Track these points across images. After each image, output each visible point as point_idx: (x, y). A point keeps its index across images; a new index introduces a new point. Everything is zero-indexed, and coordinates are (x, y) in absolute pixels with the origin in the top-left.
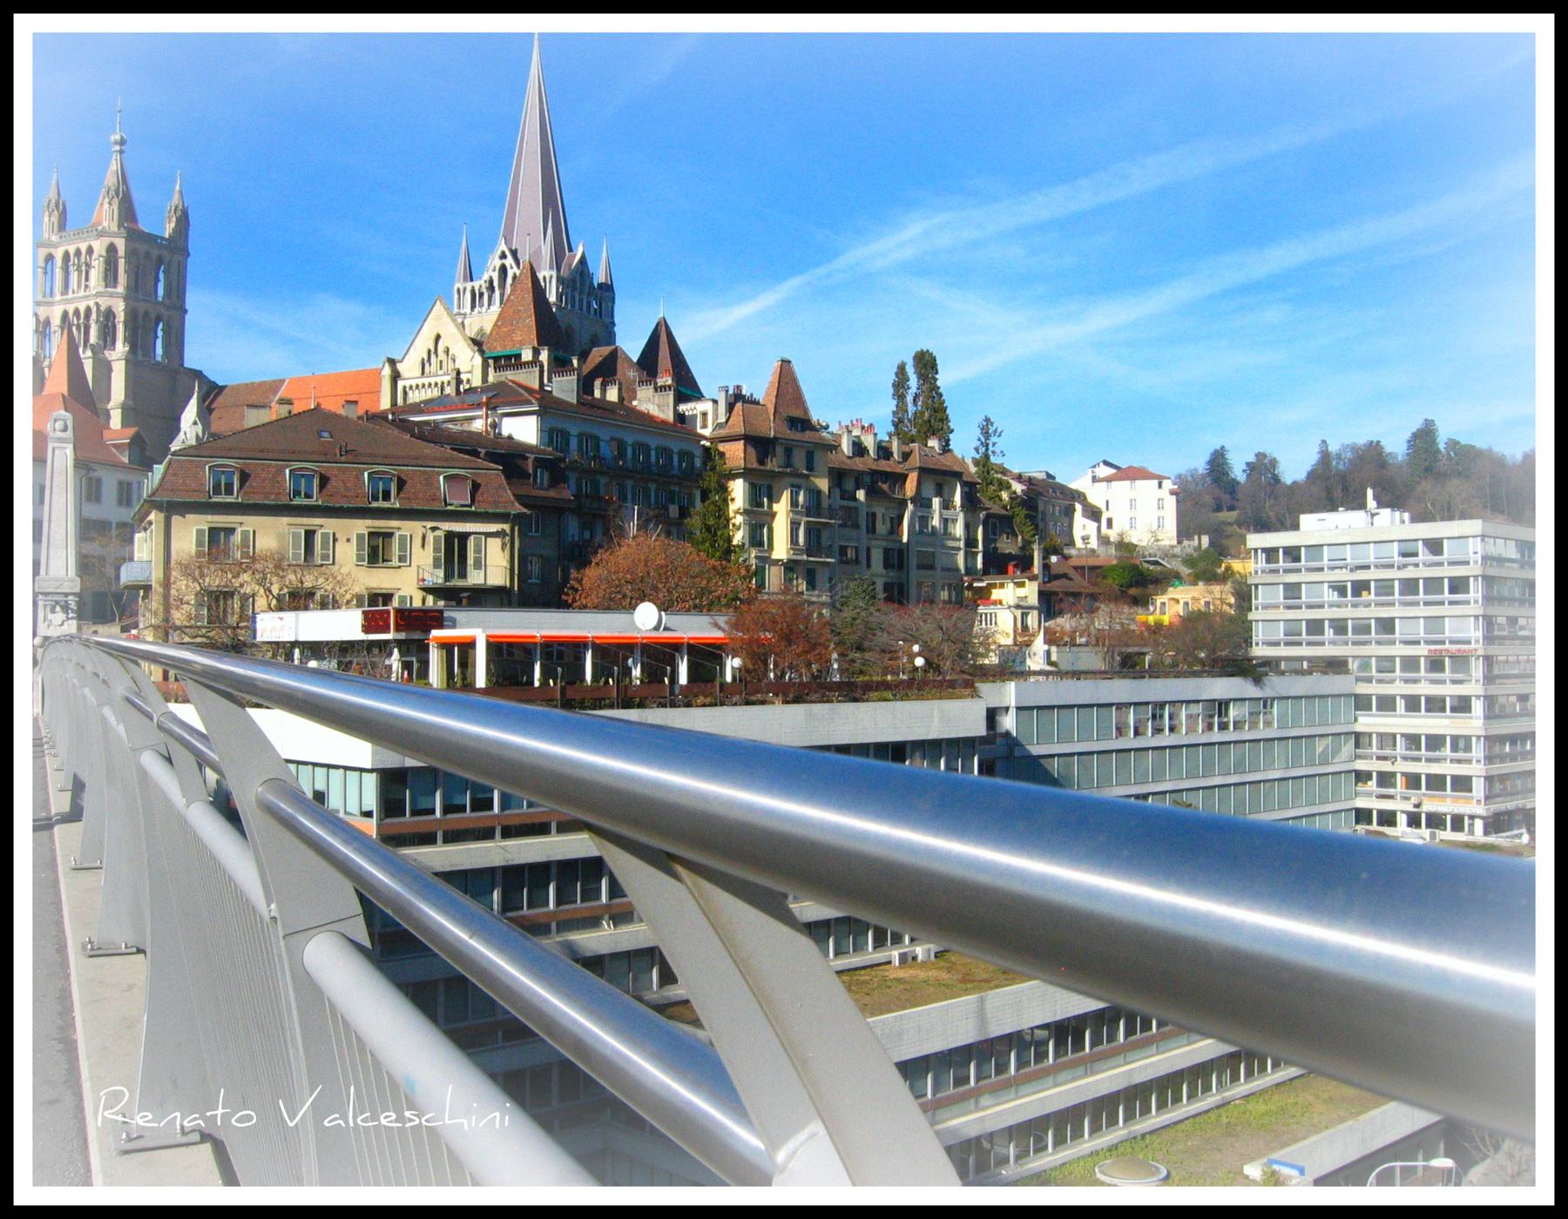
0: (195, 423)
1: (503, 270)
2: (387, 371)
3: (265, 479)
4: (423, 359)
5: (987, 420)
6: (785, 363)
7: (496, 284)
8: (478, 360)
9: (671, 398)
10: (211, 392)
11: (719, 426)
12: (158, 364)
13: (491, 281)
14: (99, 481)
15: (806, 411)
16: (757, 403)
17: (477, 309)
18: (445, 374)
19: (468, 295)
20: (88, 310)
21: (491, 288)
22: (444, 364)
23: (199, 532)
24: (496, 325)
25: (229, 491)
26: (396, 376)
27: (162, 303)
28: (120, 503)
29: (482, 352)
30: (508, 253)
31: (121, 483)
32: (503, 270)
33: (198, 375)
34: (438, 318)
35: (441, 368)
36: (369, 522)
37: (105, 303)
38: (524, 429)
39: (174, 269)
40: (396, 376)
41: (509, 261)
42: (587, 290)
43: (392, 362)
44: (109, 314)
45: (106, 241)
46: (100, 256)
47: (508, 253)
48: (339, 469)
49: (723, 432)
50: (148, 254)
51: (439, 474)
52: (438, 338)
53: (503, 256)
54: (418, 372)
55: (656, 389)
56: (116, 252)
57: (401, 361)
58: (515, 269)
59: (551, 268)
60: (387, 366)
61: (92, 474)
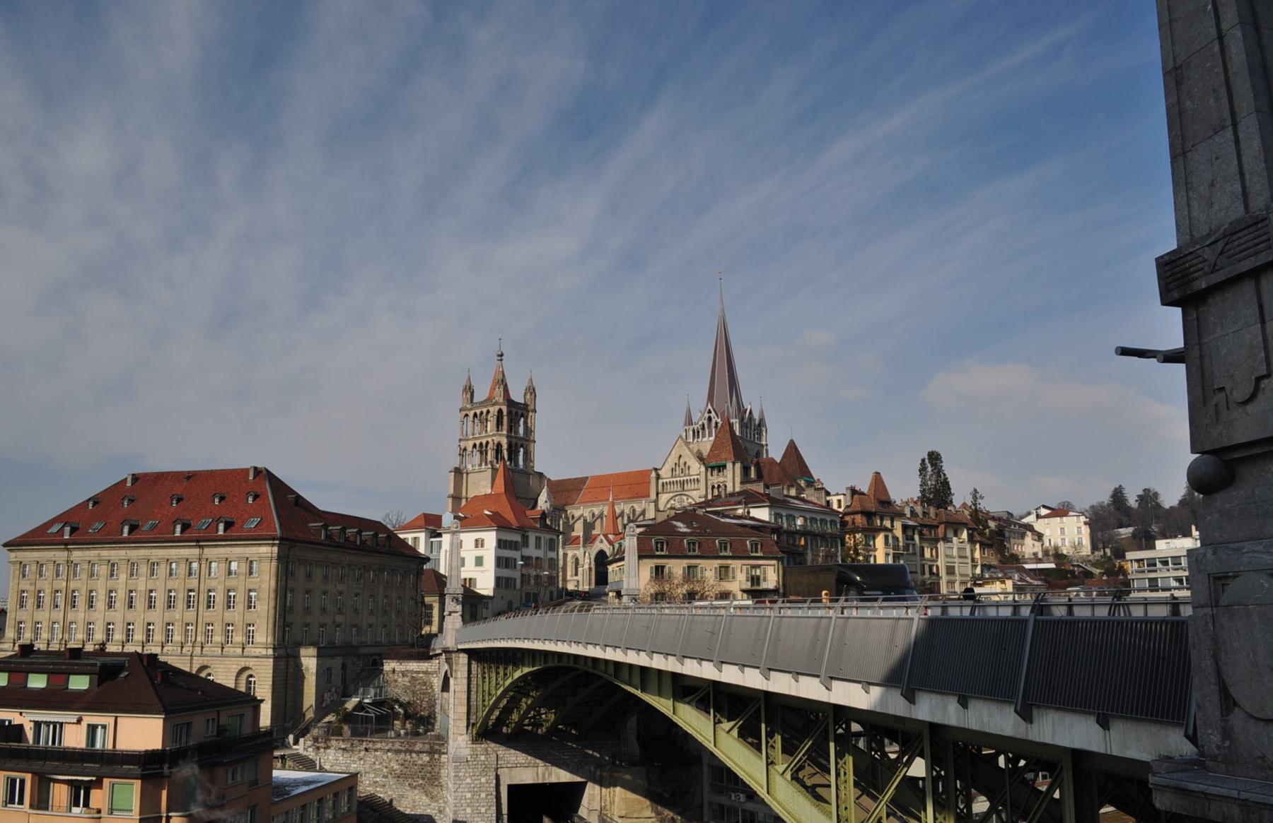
0: (546, 502)
1: (710, 419)
2: (653, 474)
4: (673, 469)
5: (975, 490)
6: (878, 474)
7: (706, 426)
8: (703, 469)
9: (823, 493)
12: (521, 470)
13: (703, 425)
14: (527, 537)
15: (889, 497)
16: (863, 494)
17: (696, 440)
18: (685, 476)
19: (691, 433)
20: (487, 443)
23: (652, 568)
24: (711, 450)
25: (662, 550)
26: (658, 477)
27: (521, 439)
28: (536, 548)
30: (712, 410)
31: (536, 537)
32: (710, 419)
33: (541, 475)
34: (680, 447)
35: (682, 472)
36: (719, 561)
37: (496, 439)
40: (658, 477)
41: (713, 414)
43: (656, 470)
44: (499, 445)
45: (497, 408)
46: (494, 415)
47: (712, 410)
49: (849, 510)
51: (747, 540)
52: (680, 456)
55: (815, 489)
57: (660, 469)
58: (716, 419)
61: (527, 534)
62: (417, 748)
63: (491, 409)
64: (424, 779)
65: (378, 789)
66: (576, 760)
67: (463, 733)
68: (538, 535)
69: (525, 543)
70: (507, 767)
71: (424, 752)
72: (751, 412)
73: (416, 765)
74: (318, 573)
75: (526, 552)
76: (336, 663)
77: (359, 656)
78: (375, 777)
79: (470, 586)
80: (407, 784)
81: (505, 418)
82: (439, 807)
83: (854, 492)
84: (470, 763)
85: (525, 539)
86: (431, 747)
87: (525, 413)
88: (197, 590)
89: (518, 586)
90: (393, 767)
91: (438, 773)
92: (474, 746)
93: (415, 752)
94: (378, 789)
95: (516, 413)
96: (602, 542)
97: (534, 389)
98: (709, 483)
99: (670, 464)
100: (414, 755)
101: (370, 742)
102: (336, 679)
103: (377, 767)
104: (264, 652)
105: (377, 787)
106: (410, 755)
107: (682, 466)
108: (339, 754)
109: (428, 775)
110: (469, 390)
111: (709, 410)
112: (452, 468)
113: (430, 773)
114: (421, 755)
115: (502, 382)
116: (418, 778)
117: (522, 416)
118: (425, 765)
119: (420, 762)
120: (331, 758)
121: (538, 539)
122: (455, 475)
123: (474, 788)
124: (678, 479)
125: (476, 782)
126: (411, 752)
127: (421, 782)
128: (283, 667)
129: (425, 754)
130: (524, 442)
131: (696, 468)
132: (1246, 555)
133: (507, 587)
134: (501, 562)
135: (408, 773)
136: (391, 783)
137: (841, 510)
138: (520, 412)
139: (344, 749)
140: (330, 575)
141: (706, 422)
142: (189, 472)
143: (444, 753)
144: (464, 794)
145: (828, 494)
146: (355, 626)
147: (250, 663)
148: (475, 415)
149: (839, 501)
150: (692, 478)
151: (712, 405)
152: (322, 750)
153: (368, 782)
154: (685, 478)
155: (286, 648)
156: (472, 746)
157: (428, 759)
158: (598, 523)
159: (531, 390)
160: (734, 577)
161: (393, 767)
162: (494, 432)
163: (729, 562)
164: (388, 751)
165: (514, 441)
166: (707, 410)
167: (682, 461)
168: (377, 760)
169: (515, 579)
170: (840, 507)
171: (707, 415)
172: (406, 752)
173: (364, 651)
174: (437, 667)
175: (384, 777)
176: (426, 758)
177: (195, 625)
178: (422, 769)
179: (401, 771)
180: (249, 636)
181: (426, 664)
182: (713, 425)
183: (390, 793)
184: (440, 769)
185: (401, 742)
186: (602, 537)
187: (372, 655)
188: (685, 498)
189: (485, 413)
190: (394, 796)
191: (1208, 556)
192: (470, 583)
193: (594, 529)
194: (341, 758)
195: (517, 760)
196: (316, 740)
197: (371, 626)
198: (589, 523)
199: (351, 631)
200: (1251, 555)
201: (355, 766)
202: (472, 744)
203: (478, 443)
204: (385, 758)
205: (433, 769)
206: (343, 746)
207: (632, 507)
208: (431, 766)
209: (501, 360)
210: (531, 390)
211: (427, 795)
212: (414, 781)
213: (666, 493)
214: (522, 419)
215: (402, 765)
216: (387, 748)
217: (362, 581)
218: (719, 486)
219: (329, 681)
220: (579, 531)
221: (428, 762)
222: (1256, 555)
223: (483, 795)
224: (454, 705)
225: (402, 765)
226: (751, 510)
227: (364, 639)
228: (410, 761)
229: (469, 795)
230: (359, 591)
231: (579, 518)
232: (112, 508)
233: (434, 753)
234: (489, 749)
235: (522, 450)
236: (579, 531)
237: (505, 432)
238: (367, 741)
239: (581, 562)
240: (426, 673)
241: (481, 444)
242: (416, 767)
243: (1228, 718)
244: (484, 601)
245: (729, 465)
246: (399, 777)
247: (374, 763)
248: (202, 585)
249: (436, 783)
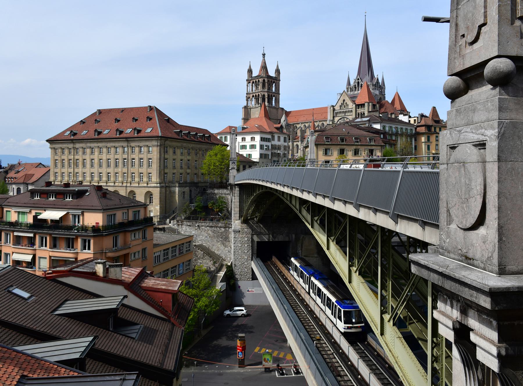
0: (284, 121)
1: (358, 83)
2: (332, 108)
3: (335, 139)
6: (434, 108)
7: (356, 86)
8: (354, 106)
10: (288, 114)
11: (418, 123)
13: (355, 85)
14: (274, 136)
15: (439, 118)
16: (427, 117)
19: (350, 89)
20: (259, 95)
21: (356, 88)
22: (346, 106)
26: (334, 110)
27: (274, 93)
28: (278, 141)
29: (355, 103)
30: (359, 79)
32: (358, 83)
33: (283, 109)
34: (344, 96)
37: (262, 93)
38: (377, 126)
39: (277, 84)
40: (334, 110)
41: (360, 81)
43: (333, 106)
44: (264, 96)
52: (344, 100)
53: (358, 79)
54: (339, 108)
56: (265, 81)
59: (370, 82)
60: (332, 108)
63: (260, 80)
64: (222, 238)
65: (203, 242)
68: (279, 135)
69: (273, 139)
72: (378, 79)
74: (178, 152)
75: (273, 143)
76: (187, 189)
77: (197, 187)
79: (249, 158)
81: (266, 84)
83: (422, 116)
85: (273, 137)
87: (275, 81)
88: (127, 159)
89: (270, 157)
95: (271, 81)
97: (279, 71)
98: (357, 112)
99: (340, 104)
100: (218, 228)
101: (200, 222)
102: (187, 196)
104: (156, 185)
107: (345, 105)
108: (187, 227)
110: (250, 71)
111: (358, 78)
112: (243, 106)
114: (221, 228)
115: (264, 67)
117: (274, 82)
119: (220, 231)
120: (184, 229)
121: (279, 137)
122: (245, 109)
123: (242, 242)
124: (343, 110)
125: (243, 240)
126: (217, 227)
128: (164, 191)
130: (275, 95)
131: (351, 106)
132: (463, 134)
133: (265, 158)
134: (261, 147)
137: (415, 124)
138: (273, 81)
139: (189, 225)
140: (184, 152)
141: (356, 84)
142: (123, 108)
144: (238, 245)
145: (410, 117)
146: (195, 174)
147: (151, 190)
148: (253, 82)
149: (415, 120)
150: (349, 110)
151: (359, 76)
152: (180, 226)
153: (199, 239)
154: (346, 110)
155: (165, 183)
157: (224, 230)
158: (308, 130)
159: (278, 71)
160: (361, 154)
162: (262, 90)
163: (359, 147)
164: (207, 226)
165: (270, 94)
167: (345, 103)
169: (268, 154)
170: (415, 123)
171: (357, 81)
173: (200, 185)
176: (223, 229)
177: (127, 173)
180: (149, 178)
182: (360, 85)
183: (208, 244)
187: (203, 186)
188: (346, 119)
189: (257, 81)
191: (448, 134)
192: (249, 156)
193: (306, 133)
194: (188, 229)
196: (178, 221)
197: (202, 174)
198: (303, 130)
199: (194, 176)
200: (465, 134)
201: (194, 232)
203: (254, 95)
204: (206, 229)
206: (189, 224)
209: (264, 57)
210: (278, 71)
211: (223, 245)
214: (274, 84)
217: (198, 155)
218: (361, 113)
219: (184, 198)
220: (299, 134)
222: (467, 134)
223: (246, 245)
225: (213, 232)
226: (372, 124)
227: (200, 180)
229: (240, 245)
230: (197, 159)
231: (299, 128)
232: (91, 124)
235: (274, 98)
236: (299, 134)
237: (266, 90)
239: (300, 147)
240: (225, 194)
241: (256, 95)
243: (450, 226)
244: (255, 164)
245: (366, 104)
248: (129, 157)
249: (227, 240)
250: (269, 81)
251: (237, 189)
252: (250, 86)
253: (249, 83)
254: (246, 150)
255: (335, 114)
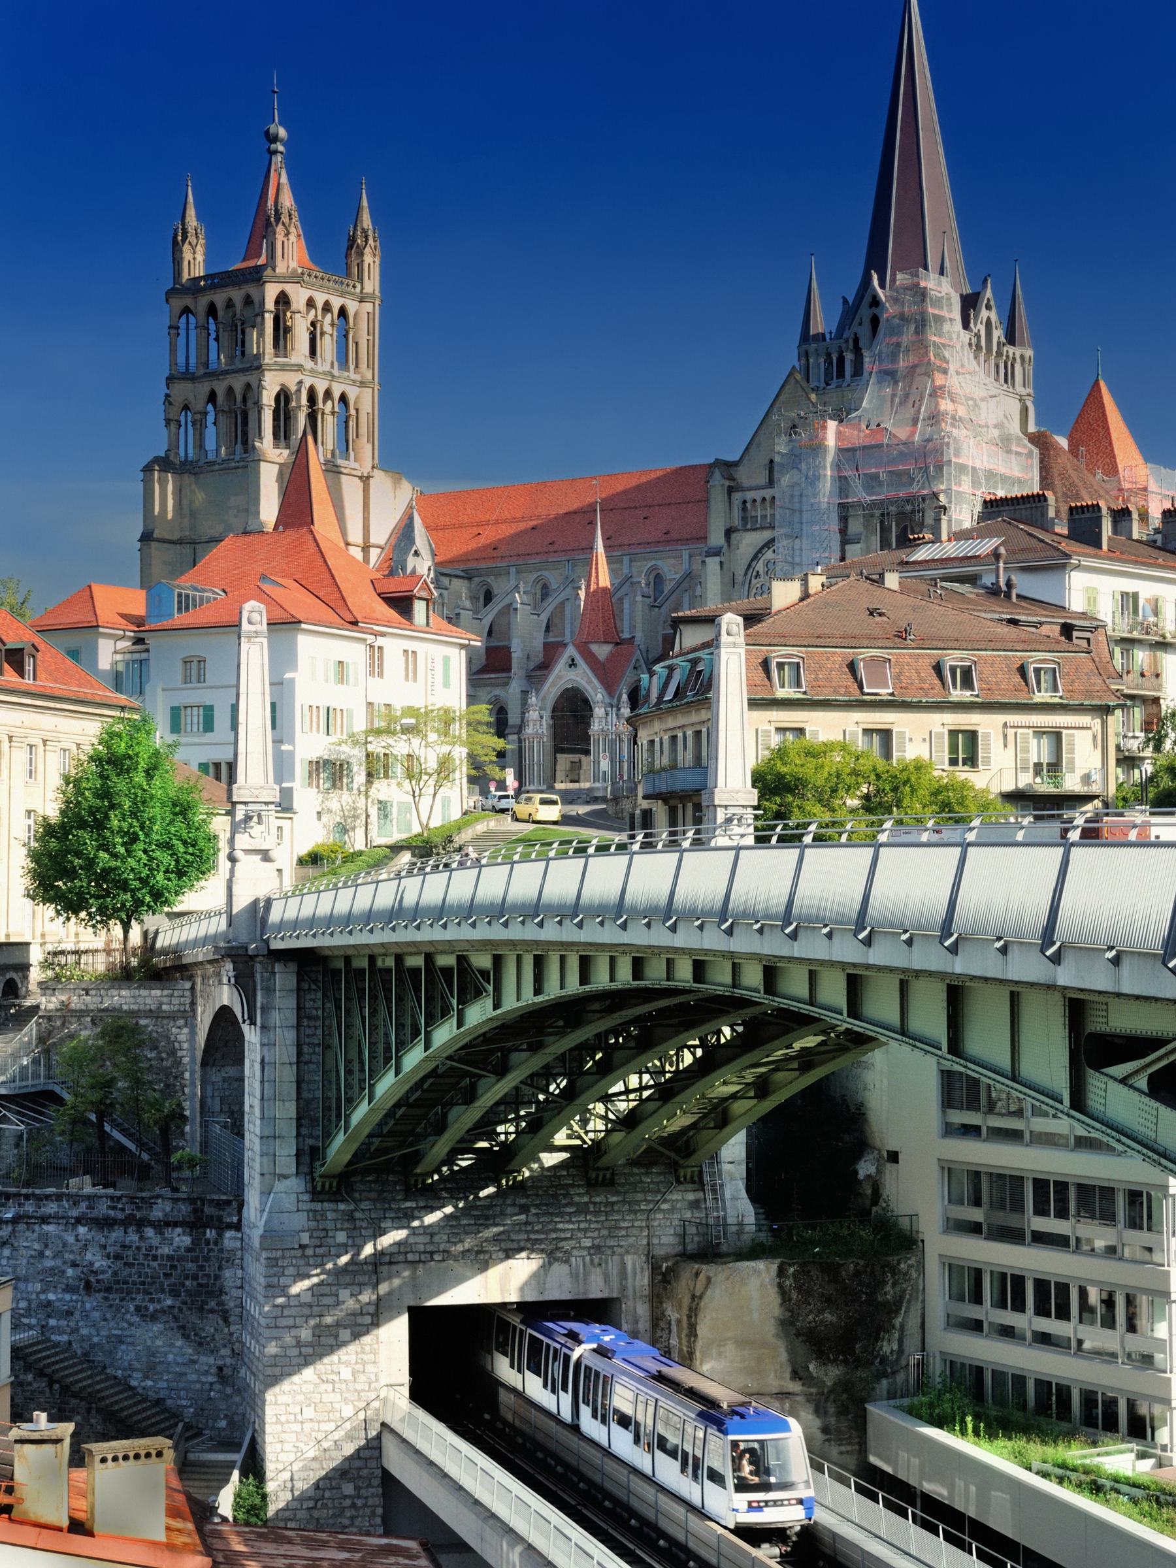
7: (861, 345)
42: (995, 348)
48: (911, 655)
50: (327, 307)
62: (157, 1213)
64: (175, 1293)
66: (587, 1243)
67: (286, 1172)
70: (406, 1262)
71: (175, 1224)
73: (155, 1258)
78: (43, 1291)
80: (132, 1308)
82: (220, 1369)
84: (309, 1252)
86: (195, 1211)
90: (92, 1264)
91: (217, 1277)
92: (318, 1206)
93: (152, 1224)
94: (52, 1322)
96: (572, 664)
100: (150, 1232)
103: (49, 1263)
105: (49, 1316)
106: (139, 1231)
109: (188, 1283)
113: (195, 1277)
114: (168, 1232)
116: (163, 1291)
118: (181, 1259)
119: (166, 1250)
127: (169, 1302)
129: (179, 1230)
135: (135, 1278)
136: (88, 1306)
143: (230, 1226)
148: (212, 310)
156: (314, 1206)
157: (187, 1240)
161: (92, 1264)
164: (79, 1221)
166: (867, 299)
168: (46, 1246)
172: (126, 1223)
174: (188, 1001)
175: (69, 1289)
176: (181, 1239)
178: (174, 1267)
179: (115, 1274)
181: (158, 992)
183: (84, 1332)
184: (220, 1268)
185: (112, 1198)
186: (571, 651)
190: (96, 1340)
195: (432, 1243)
202: (312, 1201)
204: (71, 1239)
205: (202, 1268)
207: (655, 568)
208: (195, 1260)
211: (186, 1337)
212: (152, 1300)
213: (755, 529)
215: (117, 1257)
216: (74, 1213)
221: (188, 1250)
224: (262, 1099)
225: (117, 1257)
228: (138, 1248)
233: (206, 1226)
234: (358, 1215)
238: (19, 1195)
240: (156, 1014)
242: (155, 1264)
246: (108, 1290)
247: (41, 1254)
249: (212, 1304)
250: (311, 303)
251: (284, 978)
252: (193, 334)
253: (186, 311)
254: (209, 737)
255: (737, 513)
